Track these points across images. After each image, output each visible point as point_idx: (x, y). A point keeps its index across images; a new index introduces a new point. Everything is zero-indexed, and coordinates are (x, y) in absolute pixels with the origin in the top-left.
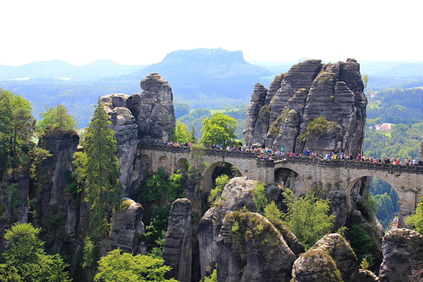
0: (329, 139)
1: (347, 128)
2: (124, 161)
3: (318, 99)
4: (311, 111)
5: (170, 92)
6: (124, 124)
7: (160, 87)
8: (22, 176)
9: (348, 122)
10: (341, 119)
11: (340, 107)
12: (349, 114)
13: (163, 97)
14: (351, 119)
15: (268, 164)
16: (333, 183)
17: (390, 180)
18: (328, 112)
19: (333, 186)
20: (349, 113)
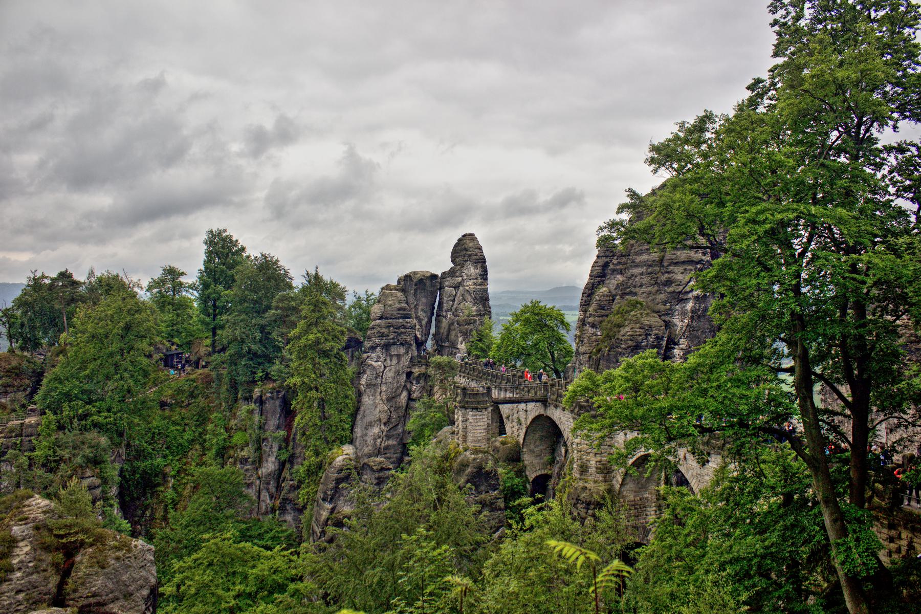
2: (374, 382)
3: (639, 259)
7: (464, 256)
8: (269, 395)
9: (684, 314)
11: (670, 275)
13: (467, 275)
14: (690, 305)
15: (467, 402)
16: (593, 463)
17: (691, 472)
18: (649, 289)
19: (592, 470)
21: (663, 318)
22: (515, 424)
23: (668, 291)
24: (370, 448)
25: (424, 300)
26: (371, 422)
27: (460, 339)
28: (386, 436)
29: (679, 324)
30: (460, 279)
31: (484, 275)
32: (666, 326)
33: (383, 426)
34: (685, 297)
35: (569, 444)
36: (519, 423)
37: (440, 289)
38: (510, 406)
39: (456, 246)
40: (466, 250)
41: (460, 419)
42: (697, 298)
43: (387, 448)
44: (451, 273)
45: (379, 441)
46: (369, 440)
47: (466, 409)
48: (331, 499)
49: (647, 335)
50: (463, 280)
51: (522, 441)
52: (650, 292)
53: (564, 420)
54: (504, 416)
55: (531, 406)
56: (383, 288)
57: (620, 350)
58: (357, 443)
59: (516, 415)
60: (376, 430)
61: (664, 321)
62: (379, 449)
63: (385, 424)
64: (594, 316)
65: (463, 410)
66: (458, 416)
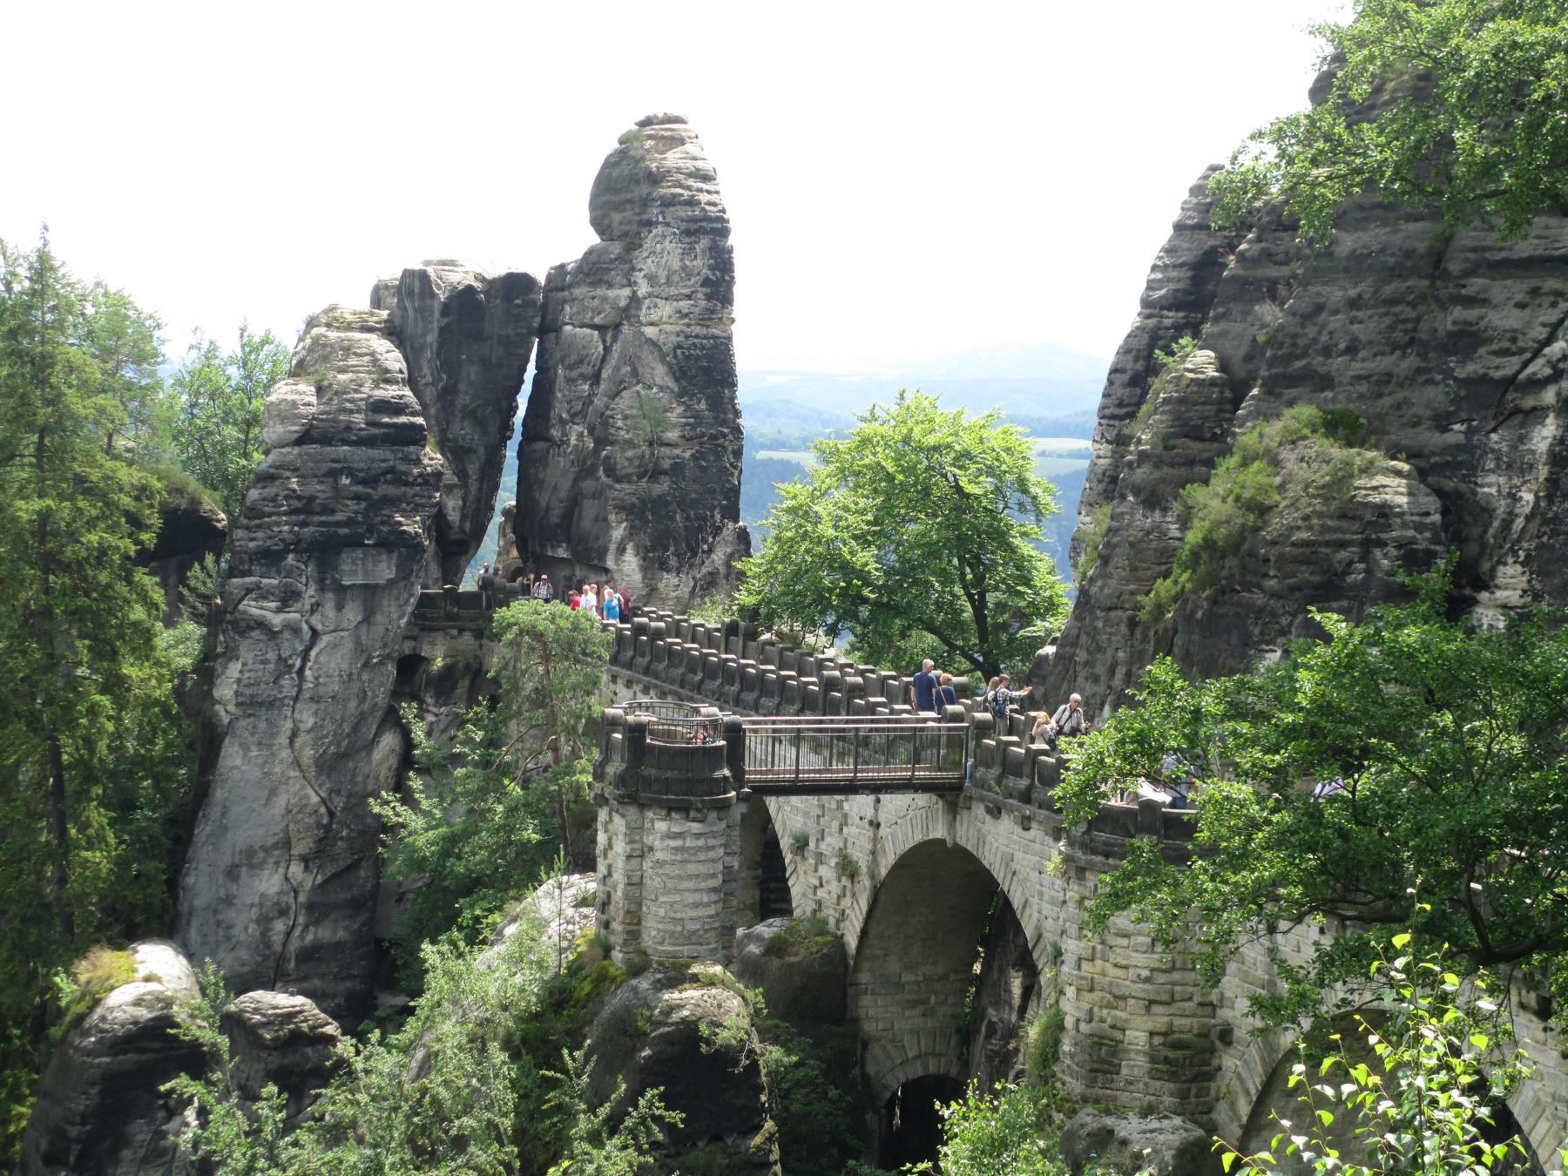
0: (1260, 612)
1: (1507, 524)
2: (265, 692)
4: (1291, 357)
5: (704, 242)
6: (303, 439)
7: (646, 202)
9: (1519, 466)
10: (1469, 433)
11: (1472, 314)
13: (651, 278)
14: (1545, 435)
15: (648, 782)
18: (1384, 363)
19: (1135, 1065)
20: (1539, 368)
21: (1432, 480)
22: (827, 872)
23: (1461, 373)
24: (244, 954)
26: (249, 853)
27: (618, 533)
28: (311, 907)
29: (1502, 506)
30: (626, 292)
31: (718, 286)
32: (1445, 512)
33: (296, 869)
34: (1529, 402)
35: (1041, 959)
36: (848, 869)
37: (542, 332)
38: (813, 800)
39: (611, 164)
40: (655, 179)
41: (620, 846)
43: (309, 955)
44: (593, 269)
45: (280, 926)
46: (244, 924)
47: (643, 807)
48: (81, 1157)
49: (1367, 546)
50: (635, 300)
51: (852, 942)
52: (1386, 378)
53: (1029, 865)
54: (785, 843)
55: (893, 803)
56: (311, 323)
57: (1258, 598)
58: (194, 935)
59: (831, 844)
60: (269, 883)
61: (1439, 492)
62: (281, 958)
63: (305, 860)
64: (1158, 463)
65: (632, 811)
66: (612, 833)
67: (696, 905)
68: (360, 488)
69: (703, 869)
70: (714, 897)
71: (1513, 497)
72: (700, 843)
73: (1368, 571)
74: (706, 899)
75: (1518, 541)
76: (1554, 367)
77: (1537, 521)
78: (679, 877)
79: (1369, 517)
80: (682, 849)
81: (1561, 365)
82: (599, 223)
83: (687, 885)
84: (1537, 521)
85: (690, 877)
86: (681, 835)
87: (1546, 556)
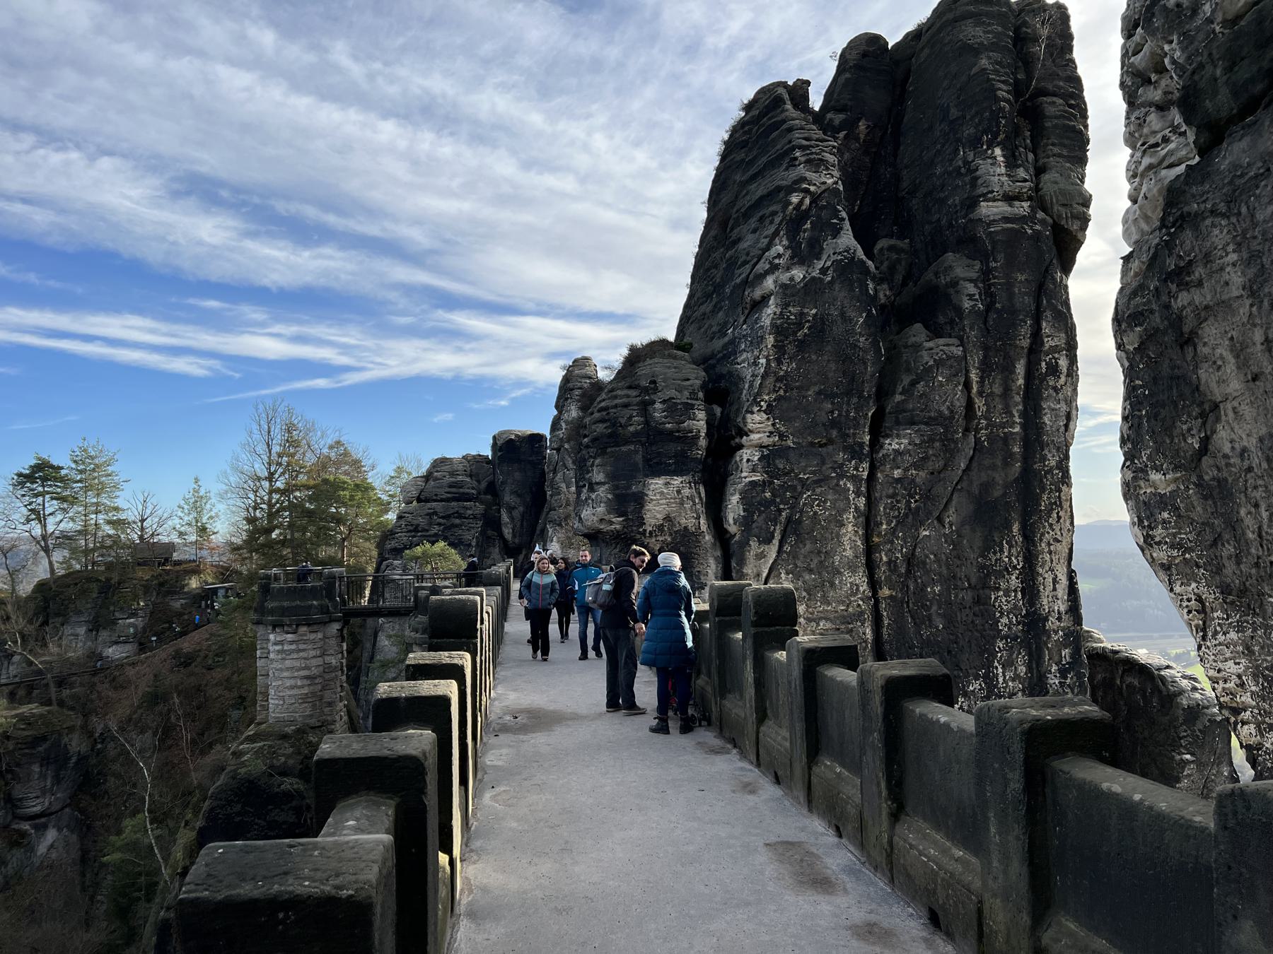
12: (762, 276)
20: (763, 266)
25: (517, 475)
34: (758, 293)
42: (786, 290)
67: (292, 687)
68: (441, 521)
69: (297, 664)
70: (307, 682)
71: (755, 364)
72: (293, 647)
73: (647, 423)
74: (299, 683)
75: (759, 394)
76: (770, 263)
77: (771, 380)
78: (281, 670)
79: (644, 383)
80: (282, 651)
81: (777, 261)
82: (557, 407)
83: (286, 674)
84: (771, 380)
85: (288, 669)
86: (281, 643)
87: (785, 405)
